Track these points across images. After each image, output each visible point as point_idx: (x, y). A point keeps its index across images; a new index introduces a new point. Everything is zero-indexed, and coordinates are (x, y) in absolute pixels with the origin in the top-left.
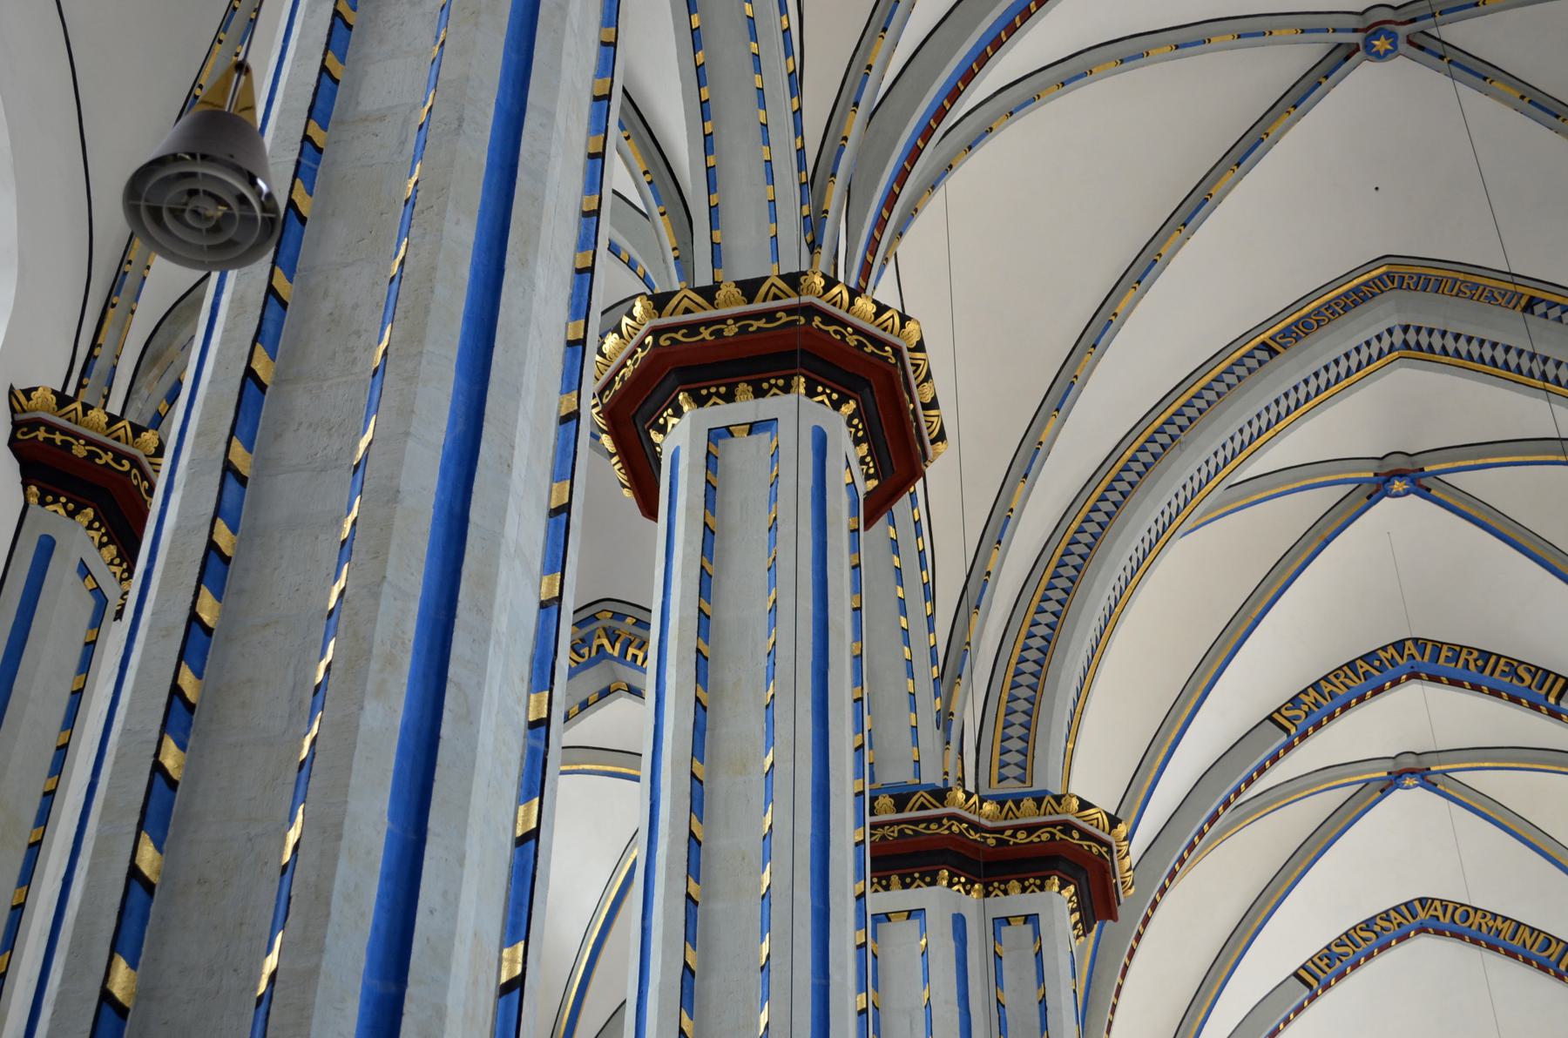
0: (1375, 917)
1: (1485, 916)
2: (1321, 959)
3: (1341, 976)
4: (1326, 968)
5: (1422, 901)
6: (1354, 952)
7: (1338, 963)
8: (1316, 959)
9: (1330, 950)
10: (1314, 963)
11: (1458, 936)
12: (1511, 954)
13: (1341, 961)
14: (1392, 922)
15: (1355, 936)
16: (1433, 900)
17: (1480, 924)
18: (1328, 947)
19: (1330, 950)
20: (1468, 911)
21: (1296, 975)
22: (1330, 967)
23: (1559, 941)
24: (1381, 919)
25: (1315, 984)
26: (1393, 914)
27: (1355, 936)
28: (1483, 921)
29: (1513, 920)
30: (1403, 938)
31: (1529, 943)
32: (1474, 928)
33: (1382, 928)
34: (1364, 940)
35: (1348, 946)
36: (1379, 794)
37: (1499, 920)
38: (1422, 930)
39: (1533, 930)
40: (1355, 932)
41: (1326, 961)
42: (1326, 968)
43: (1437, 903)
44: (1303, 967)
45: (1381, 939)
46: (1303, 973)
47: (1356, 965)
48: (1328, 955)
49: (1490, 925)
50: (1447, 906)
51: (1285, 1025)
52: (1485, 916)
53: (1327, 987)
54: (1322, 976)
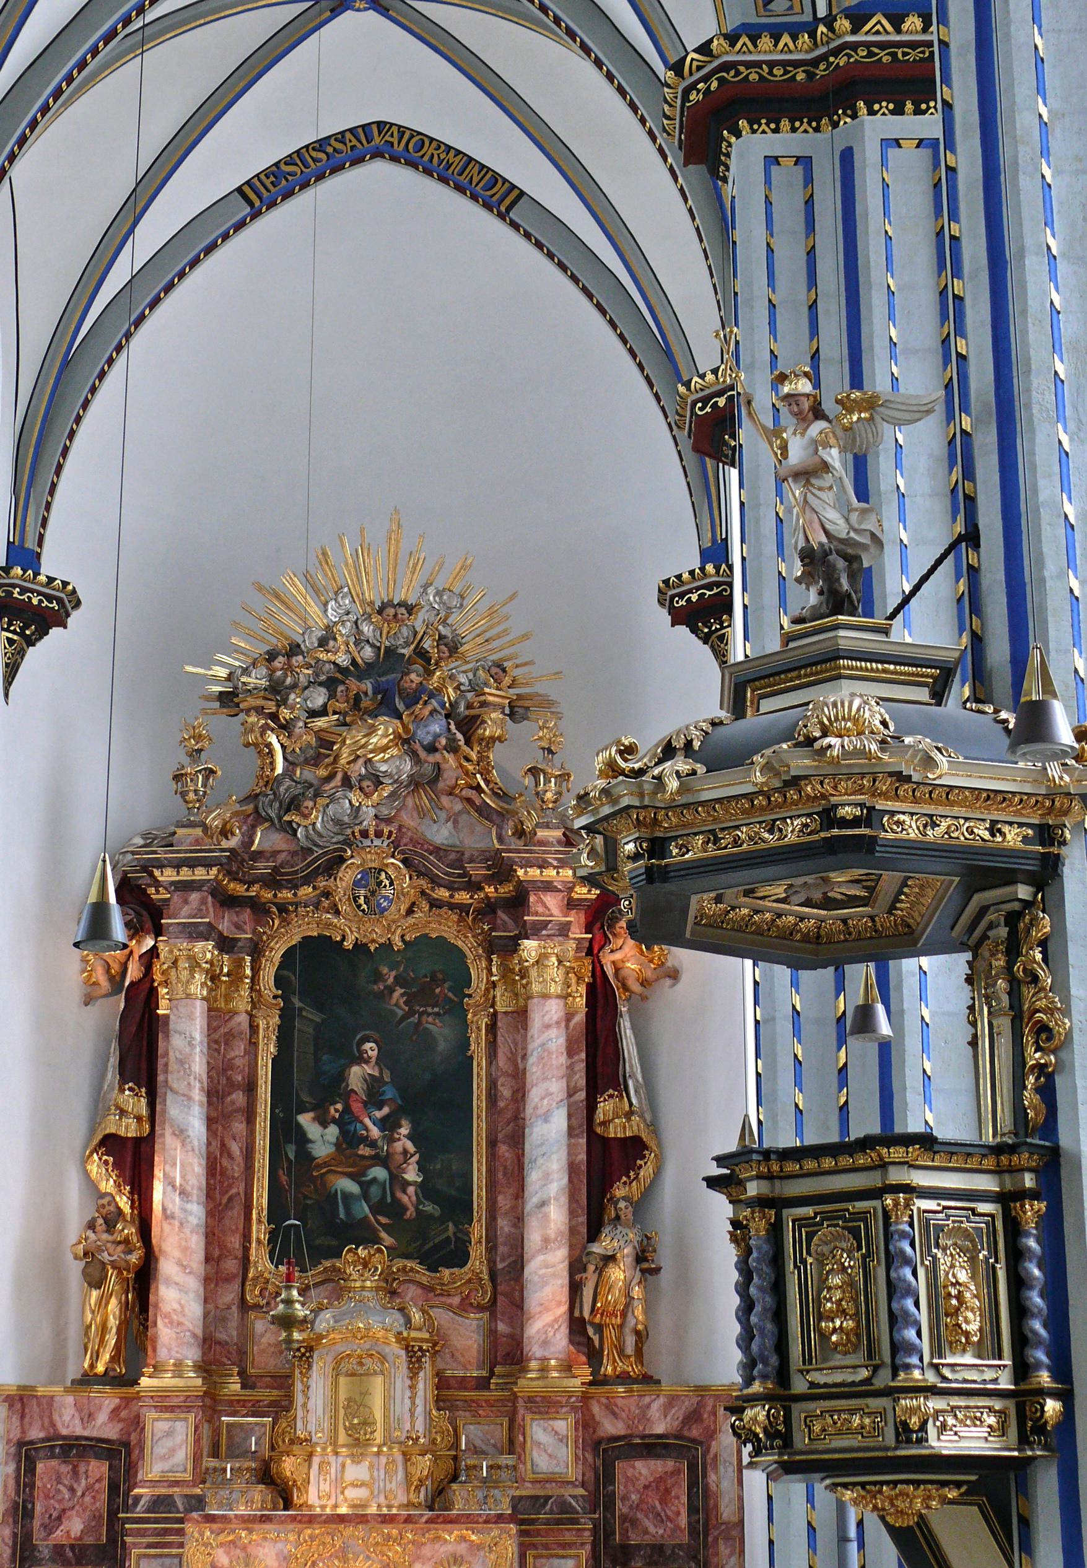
0: (330, 137)
1: (439, 148)
2: (267, 177)
3: (288, 195)
4: (270, 187)
5: (380, 124)
6: (302, 172)
7: (284, 182)
8: (262, 177)
9: (278, 168)
10: (259, 180)
11: (412, 164)
12: (460, 189)
13: (287, 180)
14: (345, 144)
15: (307, 155)
16: (392, 125)
17: (433, 155)
18: (277, 164)
19: (278, 168)
20: (423, 140)
21: (239, 190)
22: (275, 186)
23: (505, 180)
24: (336, 140)
25: (257, 204)
26: (348, 135)
27: (307, 155)
28: (436, 153)
29: (465, 155)
30: (357, 161)
31: (475, 180)
32: (426, 158)
33: (335, 150)
34: (314, 160)
35: (297, 165)
36: (328, 13)
37: (452, 152)
38: (377, 154)
39: (483, 166)
40: (307, 151)
41: (272, 178)
42: (270, 187)
43: (395, 129)
44: (248, 183)
45: (331, 161)
46: (247, 190)
47: (305, 185)
48: (275, 172)
49: (442, 156)
50: (404, 132)
51: (223, 241)
52: (439, 148)
53: (272, 205)
54: (265, 194)
